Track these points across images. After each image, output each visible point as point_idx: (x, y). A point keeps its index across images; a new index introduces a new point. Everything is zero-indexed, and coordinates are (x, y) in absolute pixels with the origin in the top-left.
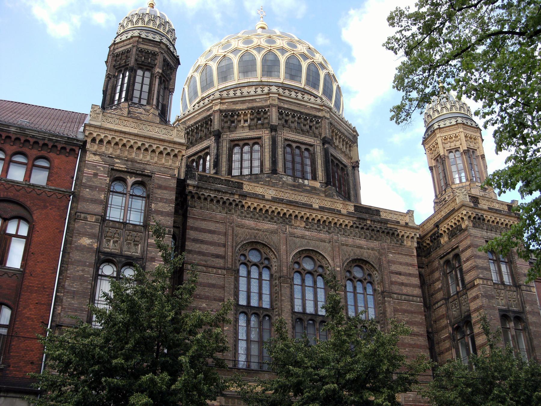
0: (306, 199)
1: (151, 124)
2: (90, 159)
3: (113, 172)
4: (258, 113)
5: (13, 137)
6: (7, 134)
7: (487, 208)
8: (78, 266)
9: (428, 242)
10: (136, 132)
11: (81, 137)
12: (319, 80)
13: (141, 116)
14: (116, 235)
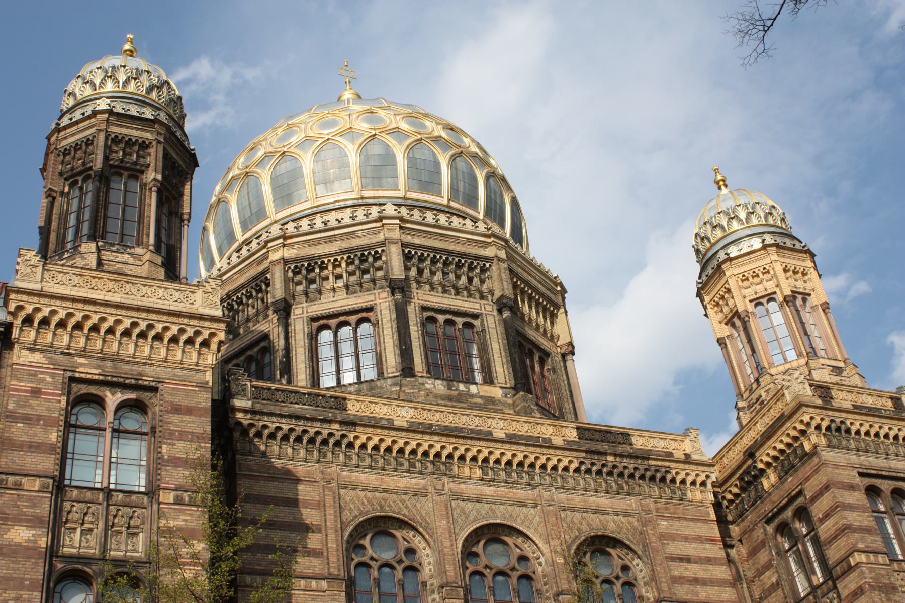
1: (150, 282)
2: (21, 361)
7: (851, 407)
10: (118, 300)
12: (476, 188)
13: (127, 270)
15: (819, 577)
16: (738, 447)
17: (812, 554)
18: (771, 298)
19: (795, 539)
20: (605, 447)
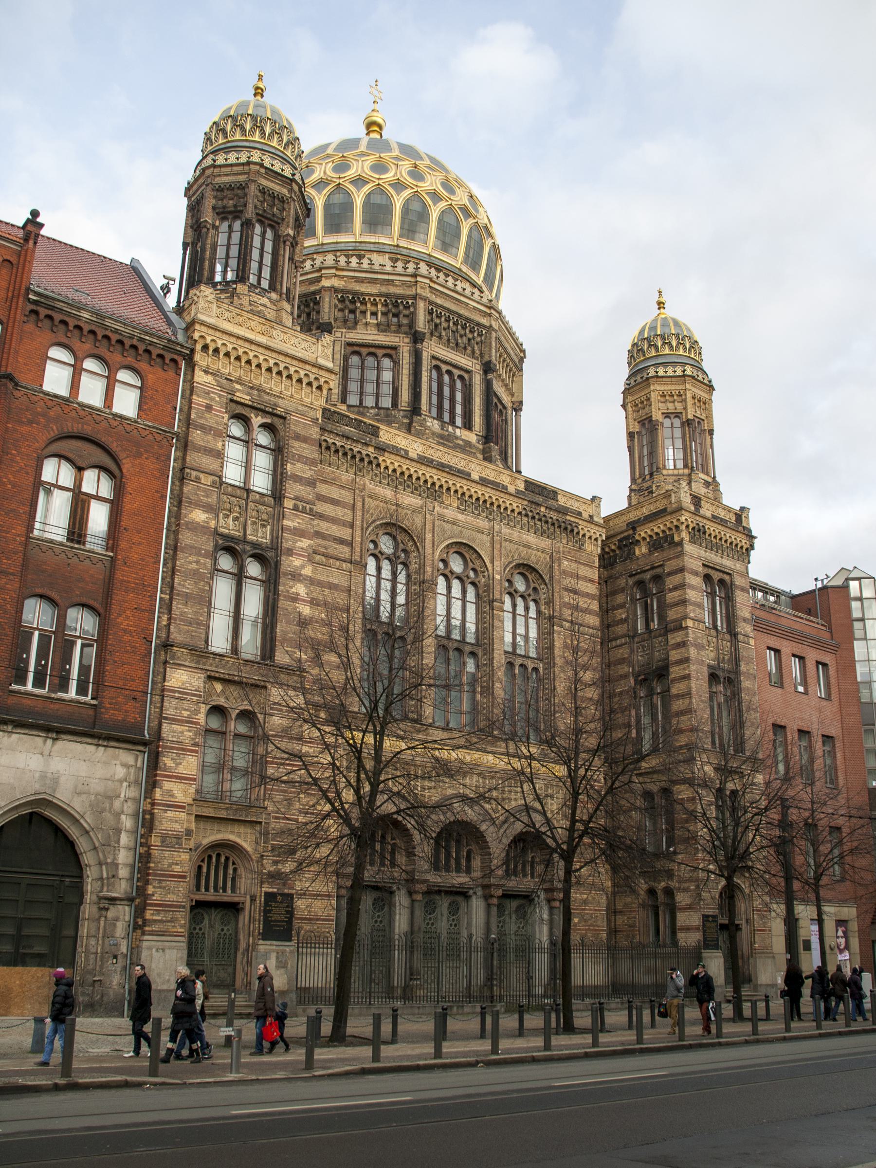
0: (463, 463)
3: (233, 405)
4: (396, 305)
5: (86, 328)
6: (77, 323)
7: (710, 516)
8: (190, 555)
9: (613, 547)
11: (181, 338)
14: (237, 509)
15: (655, 624)
16: (624, 518)
17: (655, 608)
18: (677, 415)
19: (646, 593)
20: (540, 499)
